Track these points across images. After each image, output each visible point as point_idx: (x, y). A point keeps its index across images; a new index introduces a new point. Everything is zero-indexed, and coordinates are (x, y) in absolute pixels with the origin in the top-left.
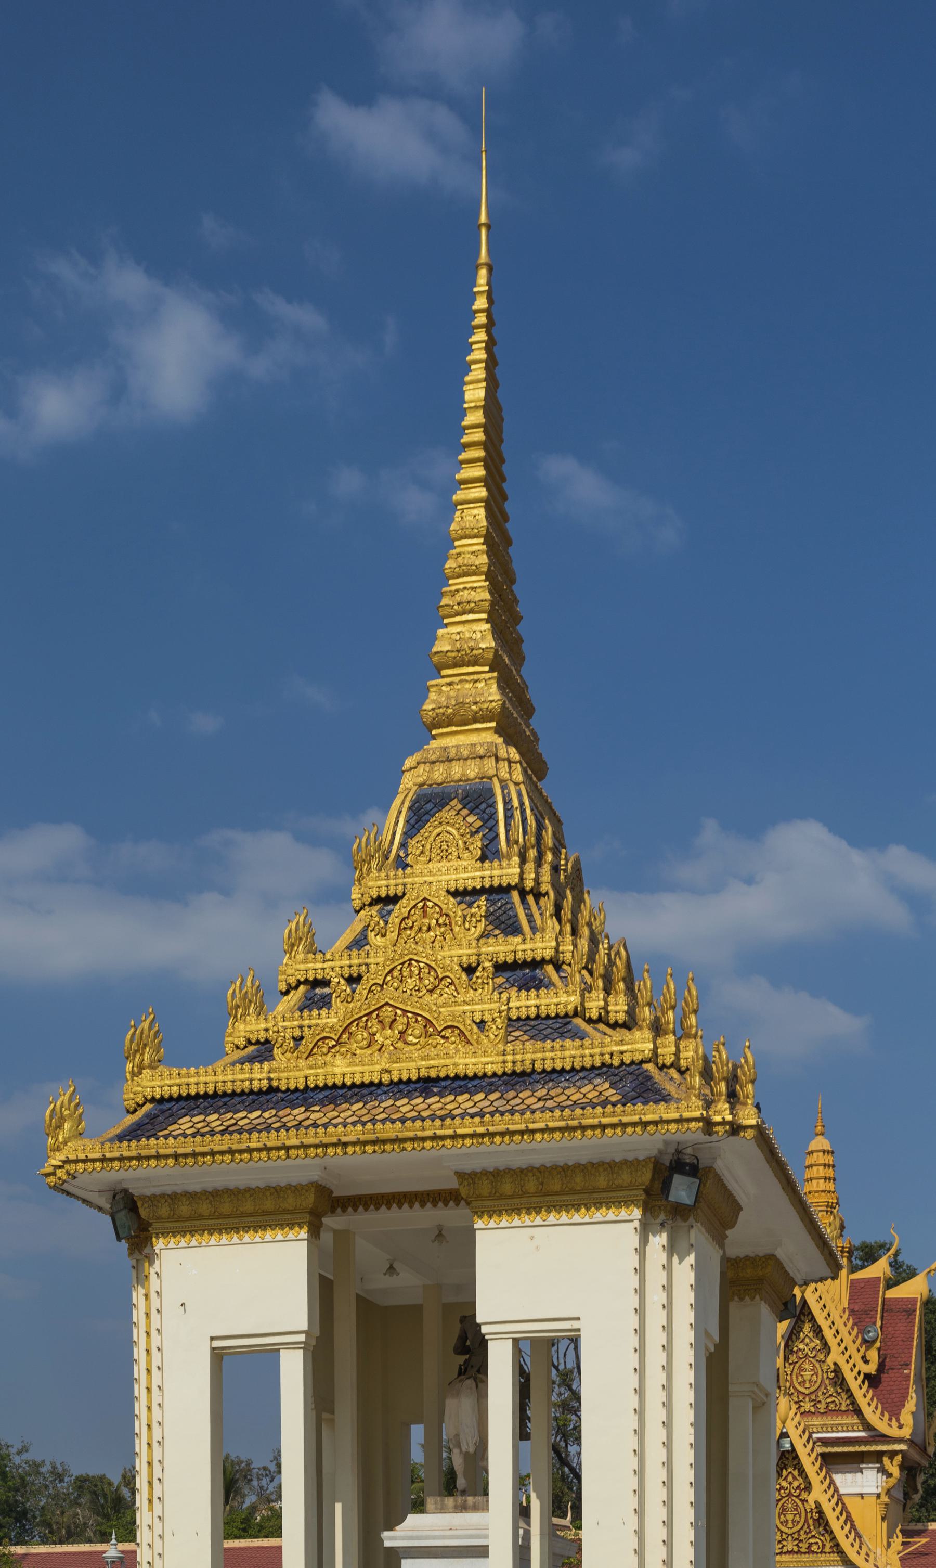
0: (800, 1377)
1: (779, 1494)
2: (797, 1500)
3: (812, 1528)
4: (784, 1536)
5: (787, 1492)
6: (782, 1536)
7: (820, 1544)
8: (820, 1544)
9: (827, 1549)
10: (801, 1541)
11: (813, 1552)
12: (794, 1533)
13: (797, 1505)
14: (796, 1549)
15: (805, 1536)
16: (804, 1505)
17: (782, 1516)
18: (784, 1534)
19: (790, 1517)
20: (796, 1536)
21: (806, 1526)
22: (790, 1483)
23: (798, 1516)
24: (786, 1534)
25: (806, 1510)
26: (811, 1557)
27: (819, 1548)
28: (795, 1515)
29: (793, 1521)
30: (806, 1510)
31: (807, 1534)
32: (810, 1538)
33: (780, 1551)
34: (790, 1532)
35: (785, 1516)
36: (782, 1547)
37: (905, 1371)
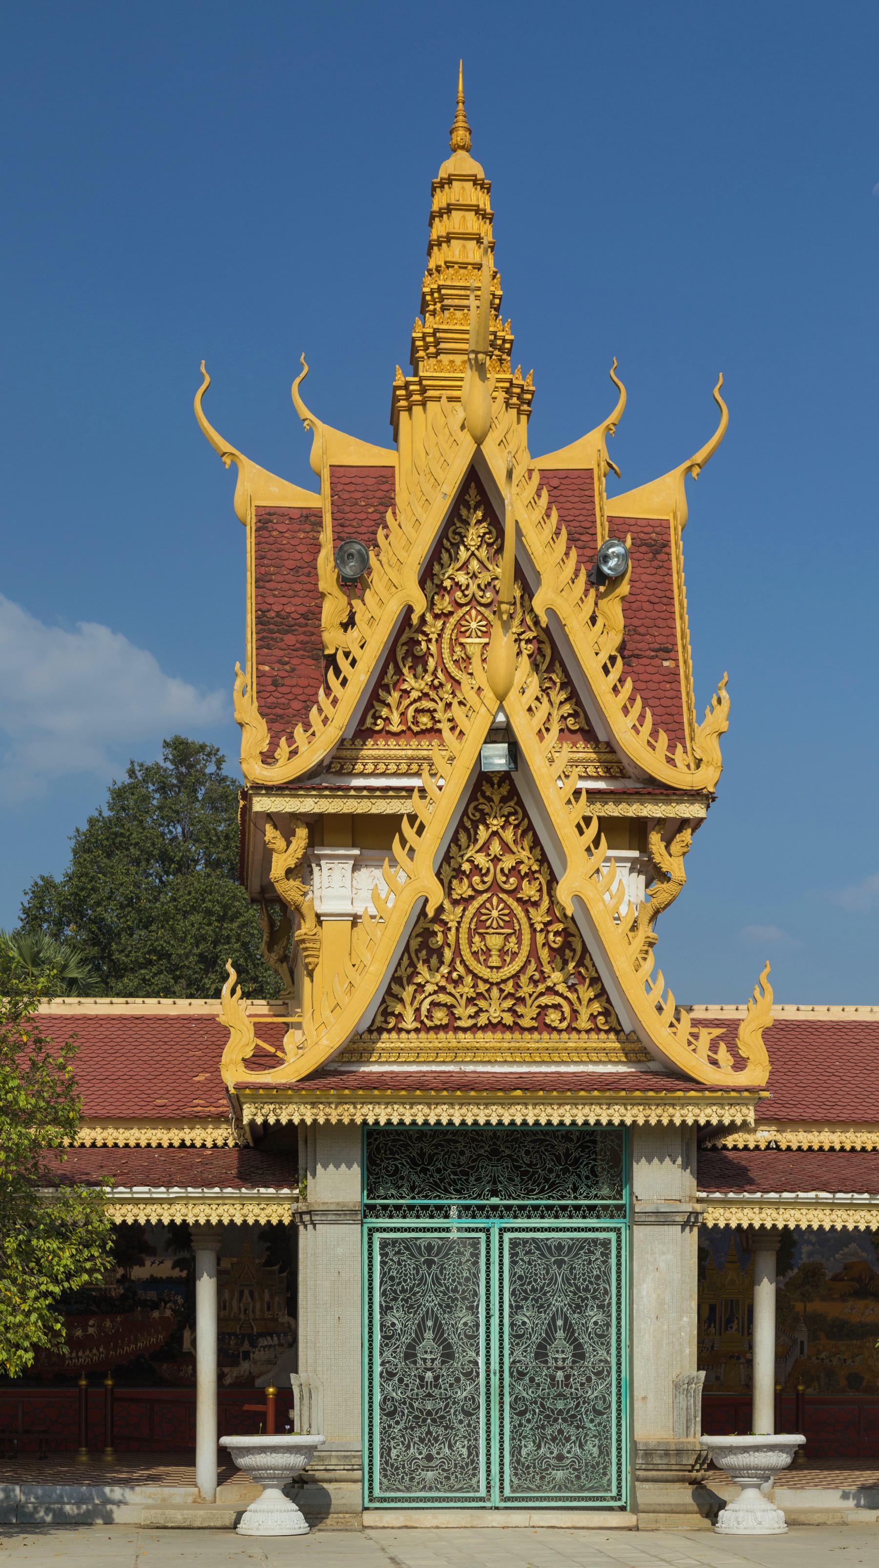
0: (458, 649)
1: (471, 885)
2: (511, 901)
3: (547, 969)
4: (482, 987)
5: (489, 879)
6: (475, 986)
7: (566, 1009)
8: (566, 1009)
9: (583, 1023)
10: (522, 1000)
11: (551, 1029)
12: (504, 981)
13: (512, 914)
14: (508, 1019)
15: (530, 989)
16: (527, 912)
17: (477, 939)
18: (480, 983)
19: (495, 942)
20: (509, 987)
21: (533, 965)
22: (496, 860)
23: (513, 939)
24: (486, 981)
25: (532, 925)
26: (546, 1040)
27: (563, 1019)
28: (510, 935)
29: (502, 952)
30: (532, 925)
31: (536, 983)
32: (542, 994)
33: (470, 1022)
34: (495, 977)
35: (483, 939)
36: (477, 1014)
37: (666, 664)
